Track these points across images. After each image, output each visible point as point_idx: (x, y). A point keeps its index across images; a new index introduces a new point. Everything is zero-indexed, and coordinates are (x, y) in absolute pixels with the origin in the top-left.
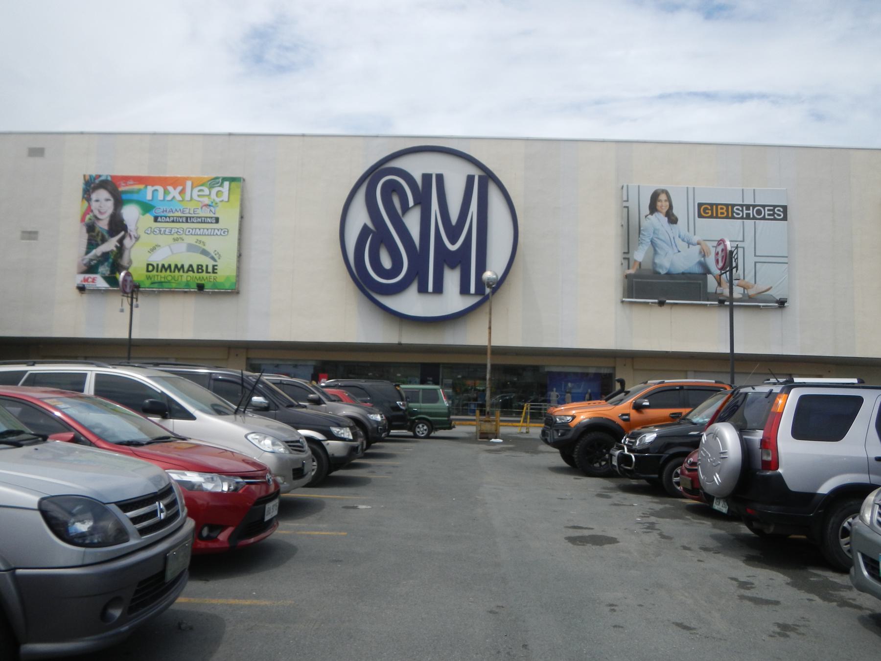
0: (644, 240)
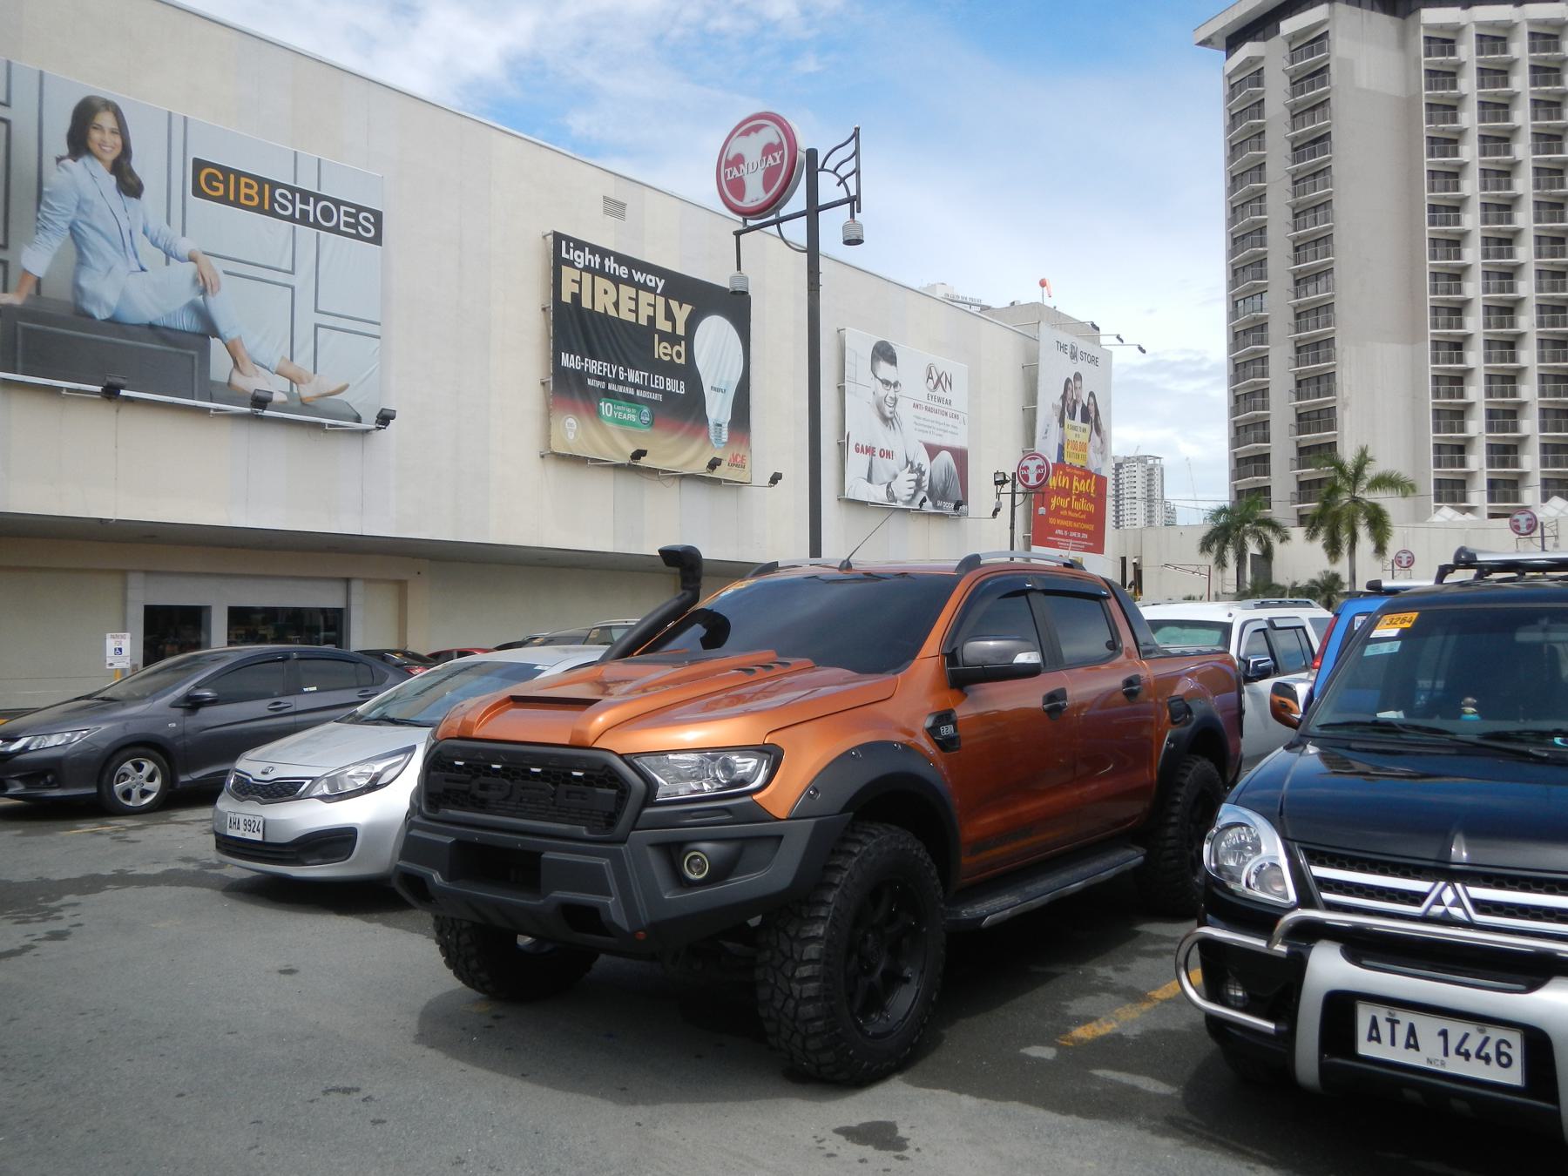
0: (53, 223)
